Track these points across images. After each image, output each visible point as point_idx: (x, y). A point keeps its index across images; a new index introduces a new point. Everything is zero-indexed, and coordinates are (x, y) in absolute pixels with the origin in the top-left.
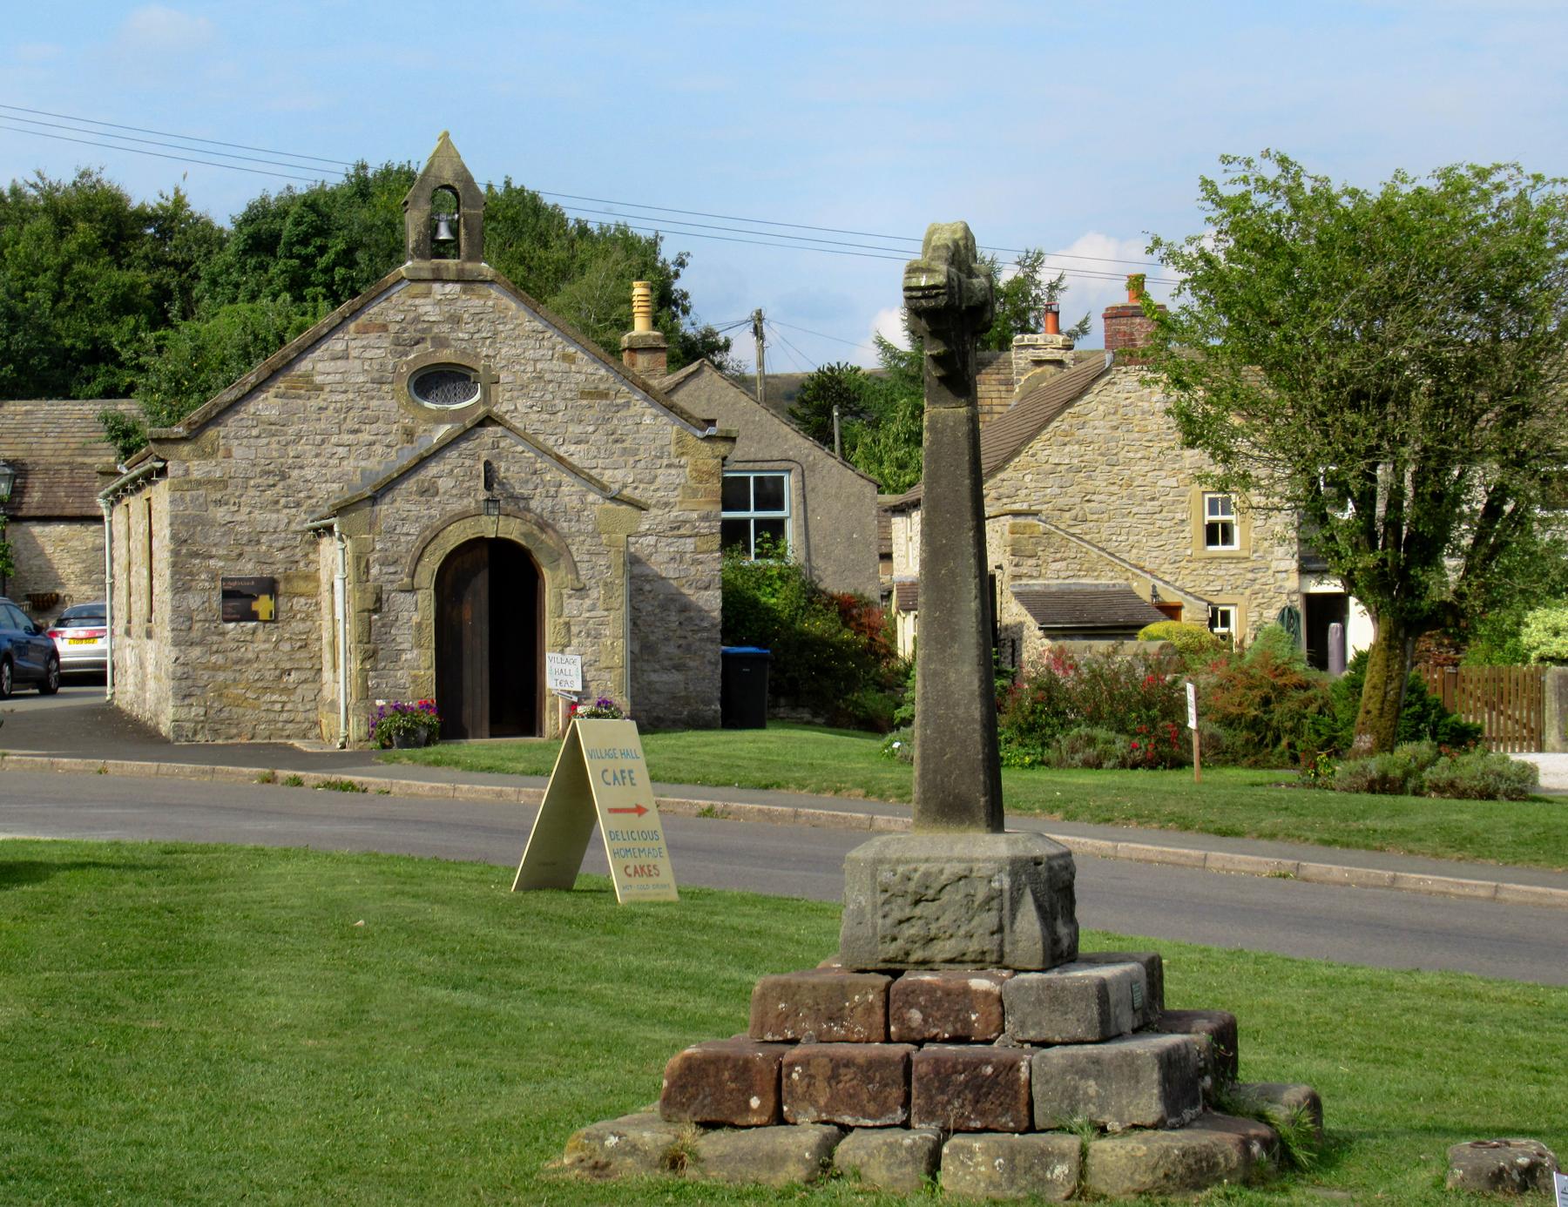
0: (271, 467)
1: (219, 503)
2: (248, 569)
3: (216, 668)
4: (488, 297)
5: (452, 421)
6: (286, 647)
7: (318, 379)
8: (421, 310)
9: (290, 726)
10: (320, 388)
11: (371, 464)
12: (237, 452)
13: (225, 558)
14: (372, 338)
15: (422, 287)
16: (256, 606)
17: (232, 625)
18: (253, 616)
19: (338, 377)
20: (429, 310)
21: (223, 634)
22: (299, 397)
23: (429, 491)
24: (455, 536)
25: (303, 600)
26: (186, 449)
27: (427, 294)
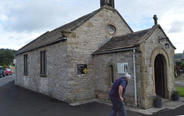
0: (85, 41)
1: (77, 48)
2: (83, 63)
3: (77, 85)
4: (116, 14)
5: (112, 35)
6: (89, 79)
7: (94, 24)
8: (108, 14)
9: (90, 96)
10: (93, 26)
11: (101, 42)
12: (80, 37)
13: (79, 60)
14: (100, 18)
15: (107, 10)
16: (84, 71)
17: (80, 75)
18: (83, 73)
19: (96, 24)
20: (109, 15)
21: (78, 77)
22: (90, 27)
23: (152, 42)
24: (156, 53)
25: (91, 69)
26: (70, 35)
27: (108, 12)
